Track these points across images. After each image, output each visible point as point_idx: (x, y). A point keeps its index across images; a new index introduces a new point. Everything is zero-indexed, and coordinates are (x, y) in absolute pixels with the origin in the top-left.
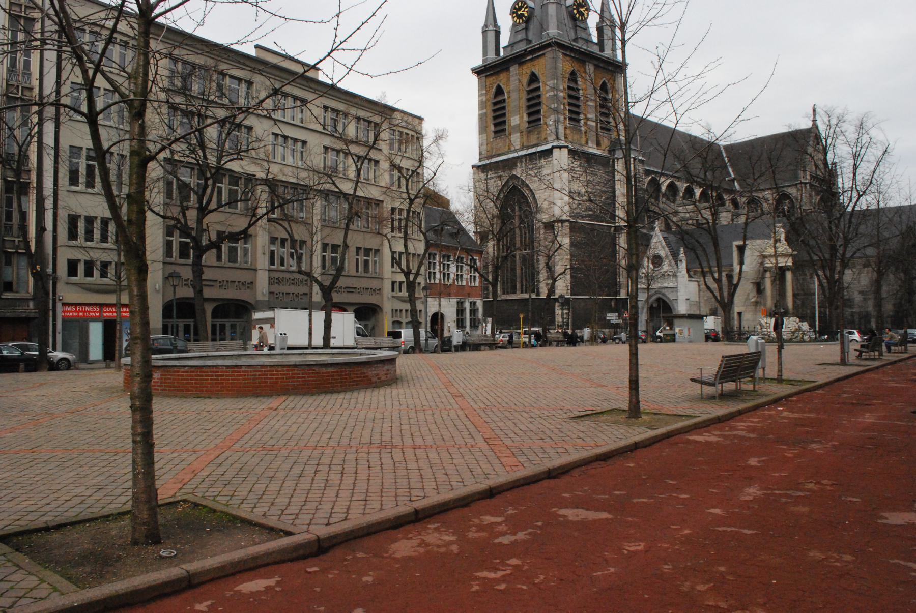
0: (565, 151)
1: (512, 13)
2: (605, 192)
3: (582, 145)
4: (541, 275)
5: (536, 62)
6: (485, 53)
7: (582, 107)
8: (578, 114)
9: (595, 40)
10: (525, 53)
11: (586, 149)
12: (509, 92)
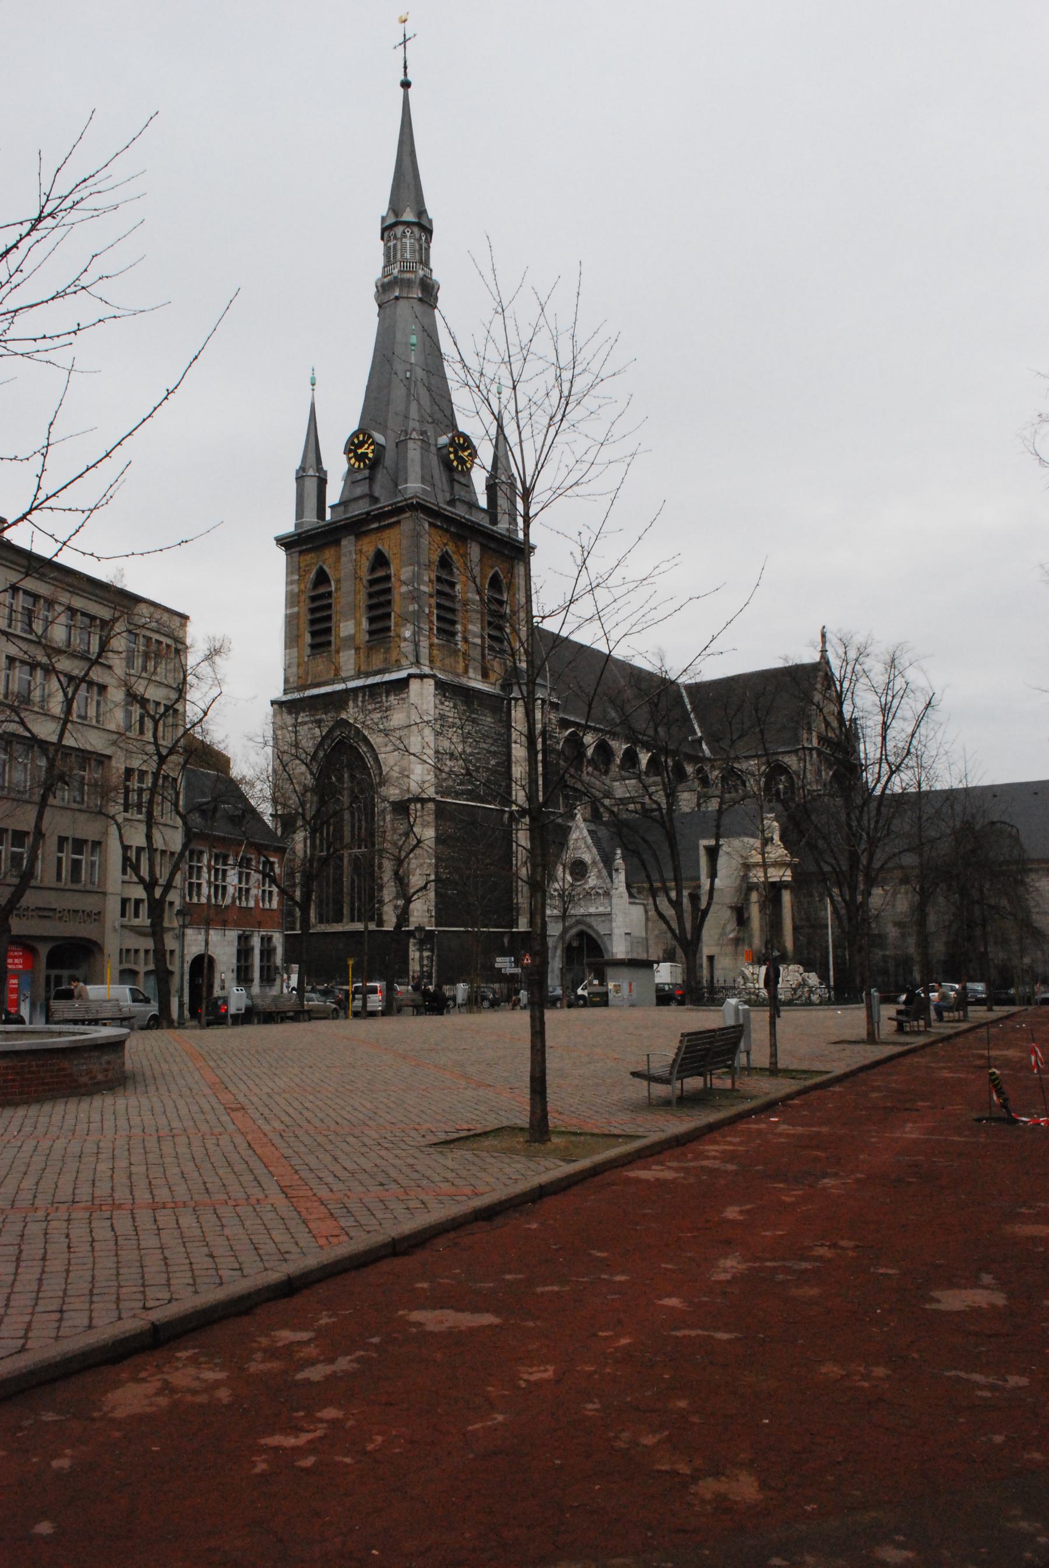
0: (432, 682)
1: (347, 451)
2: (494, 754)
3: (458, 675)
4: (385, 892)
6: (300, 513)
8: (453, 623)
9: (483, 502)
10: (368, 518)
11: (464, 681)
12: (338, 581)
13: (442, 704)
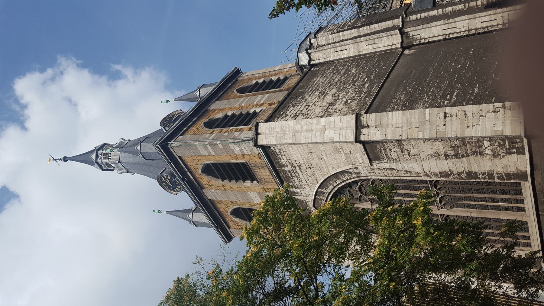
5: (192, 168)
8: (248, 113)
13: (287, 115)
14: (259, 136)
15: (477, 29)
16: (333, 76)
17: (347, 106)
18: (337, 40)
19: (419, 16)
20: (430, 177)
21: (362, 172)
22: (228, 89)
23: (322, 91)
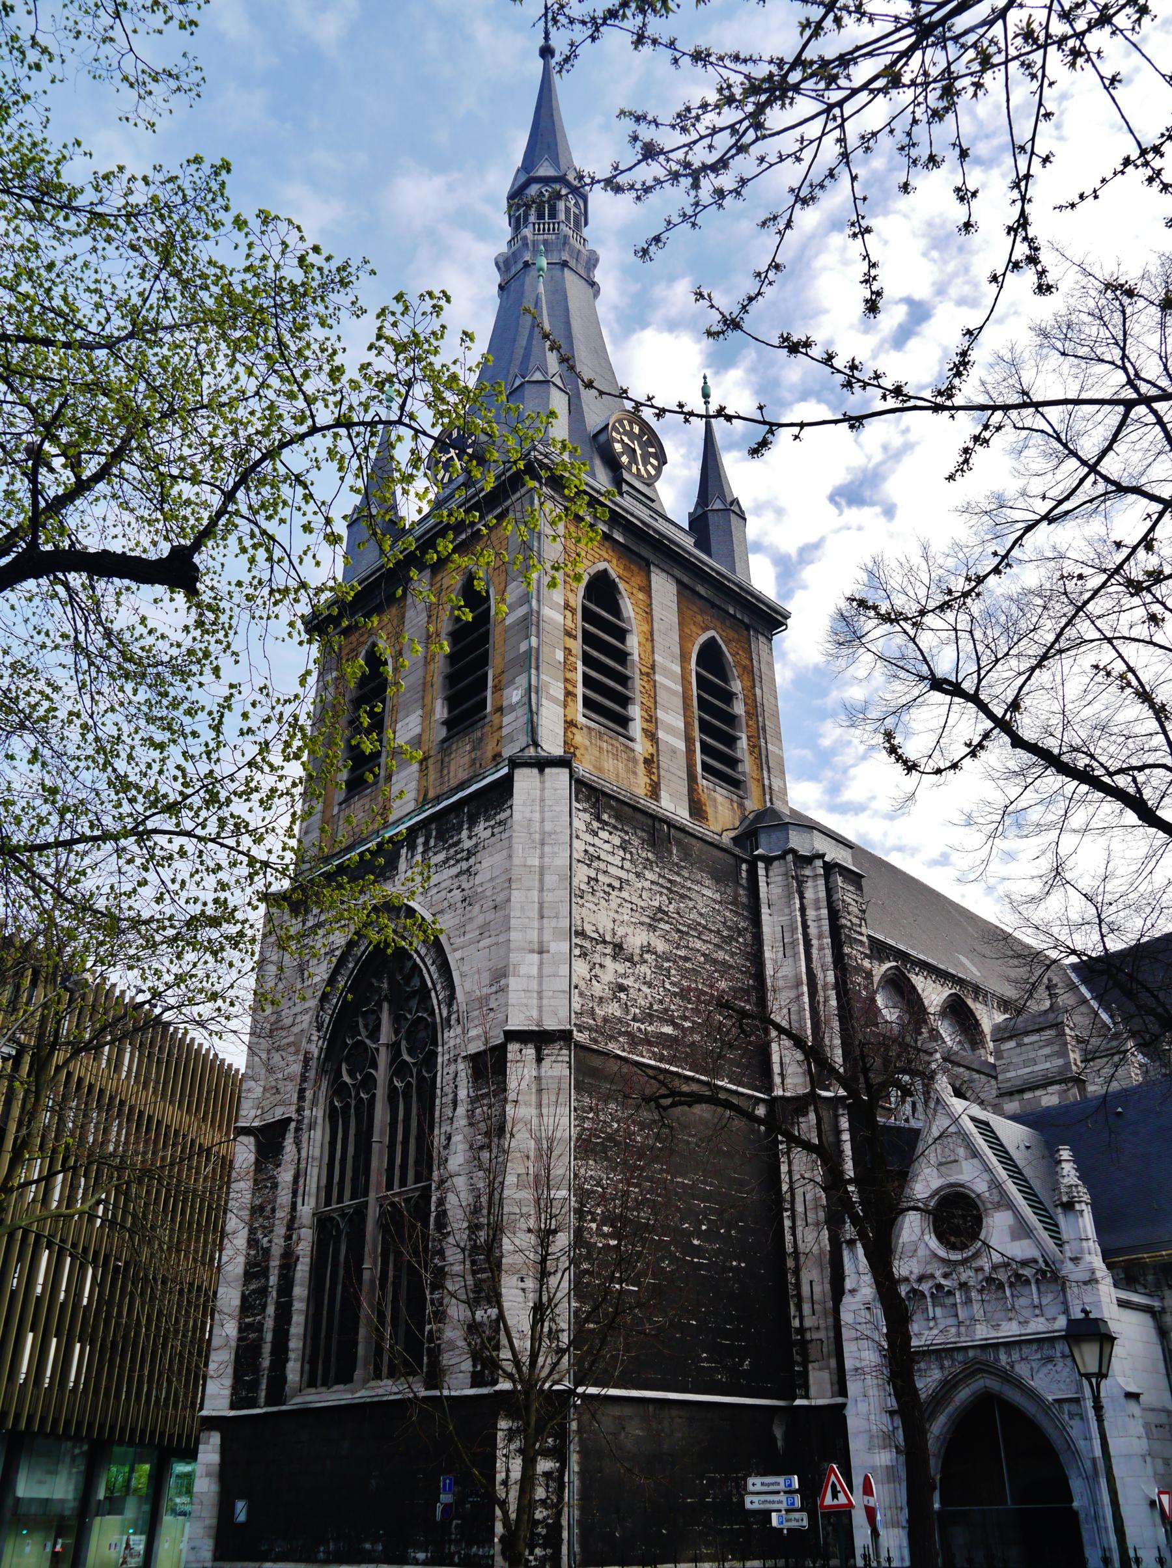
7: (638, 683)
8: (625, 701)
13: (596, 834)
14: (535, 771)
15: (797, 1272)
16: (711, 931)
17: (608, 994)
18: (813, 931)
19: (846, 1136)
20: (438, 1189)
21: (452, 1034)
22: (719, 608)
23: (665, 913)
